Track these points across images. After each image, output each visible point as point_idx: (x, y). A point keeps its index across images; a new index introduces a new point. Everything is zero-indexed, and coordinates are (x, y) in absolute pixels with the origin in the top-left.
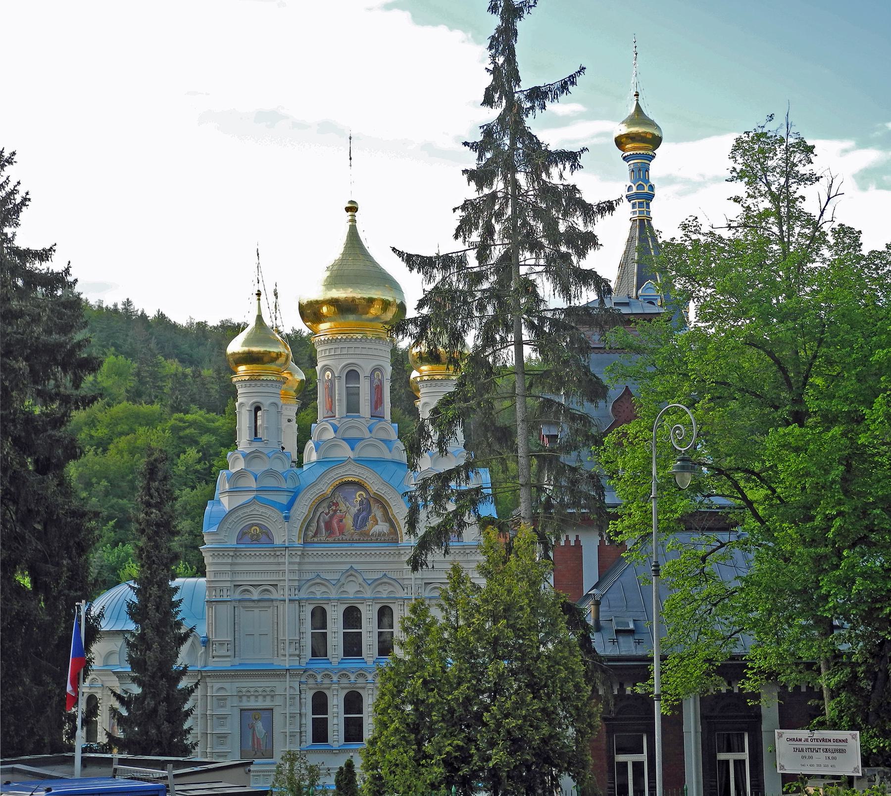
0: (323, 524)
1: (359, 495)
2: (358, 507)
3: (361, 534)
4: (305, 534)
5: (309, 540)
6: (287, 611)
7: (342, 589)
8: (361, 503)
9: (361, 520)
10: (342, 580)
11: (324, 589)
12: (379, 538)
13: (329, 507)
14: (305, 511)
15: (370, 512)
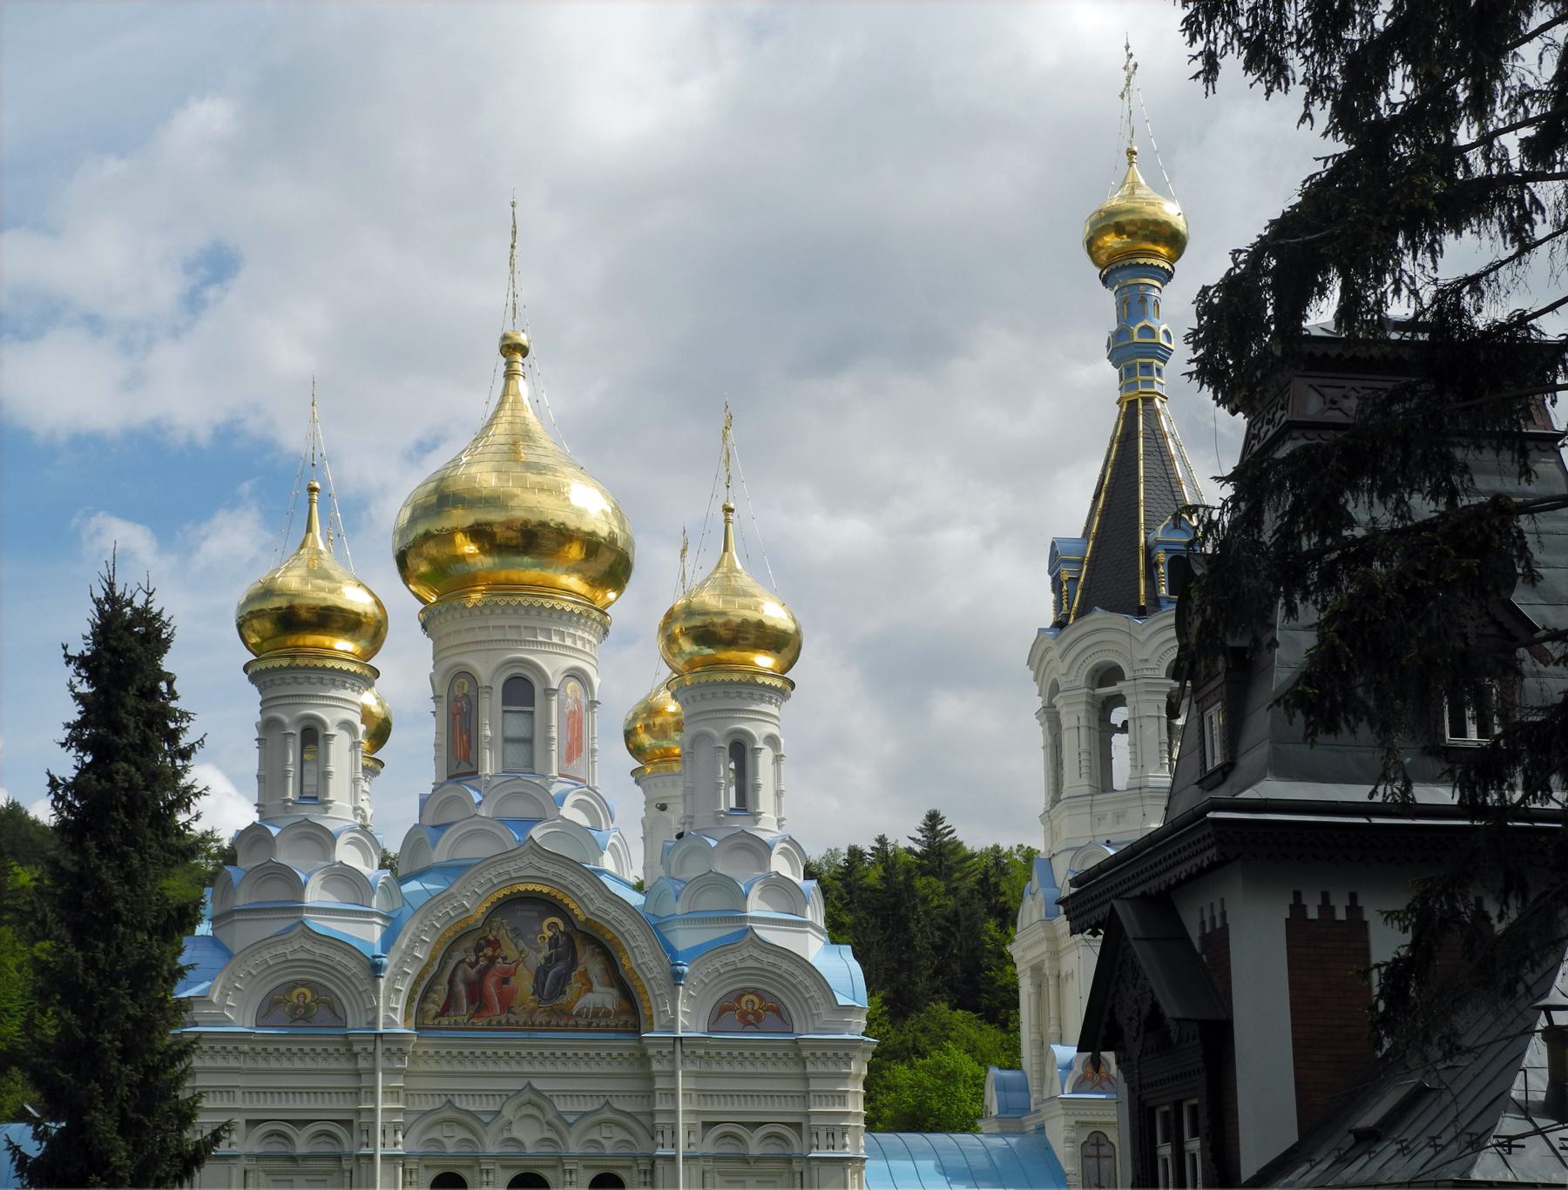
0: (461, 988)
1: (548, 927)
2: (546, 952)
3: (553, 1012)
4: (420, 1010)
5: (429, 1022)
7: (506, 1135)
8: (553, 943)
9: (552, 983)
10: (508, 1113)
11: (462, 1134)
12: (594, 1021)
13: (478, 949)
15: (574, 964)
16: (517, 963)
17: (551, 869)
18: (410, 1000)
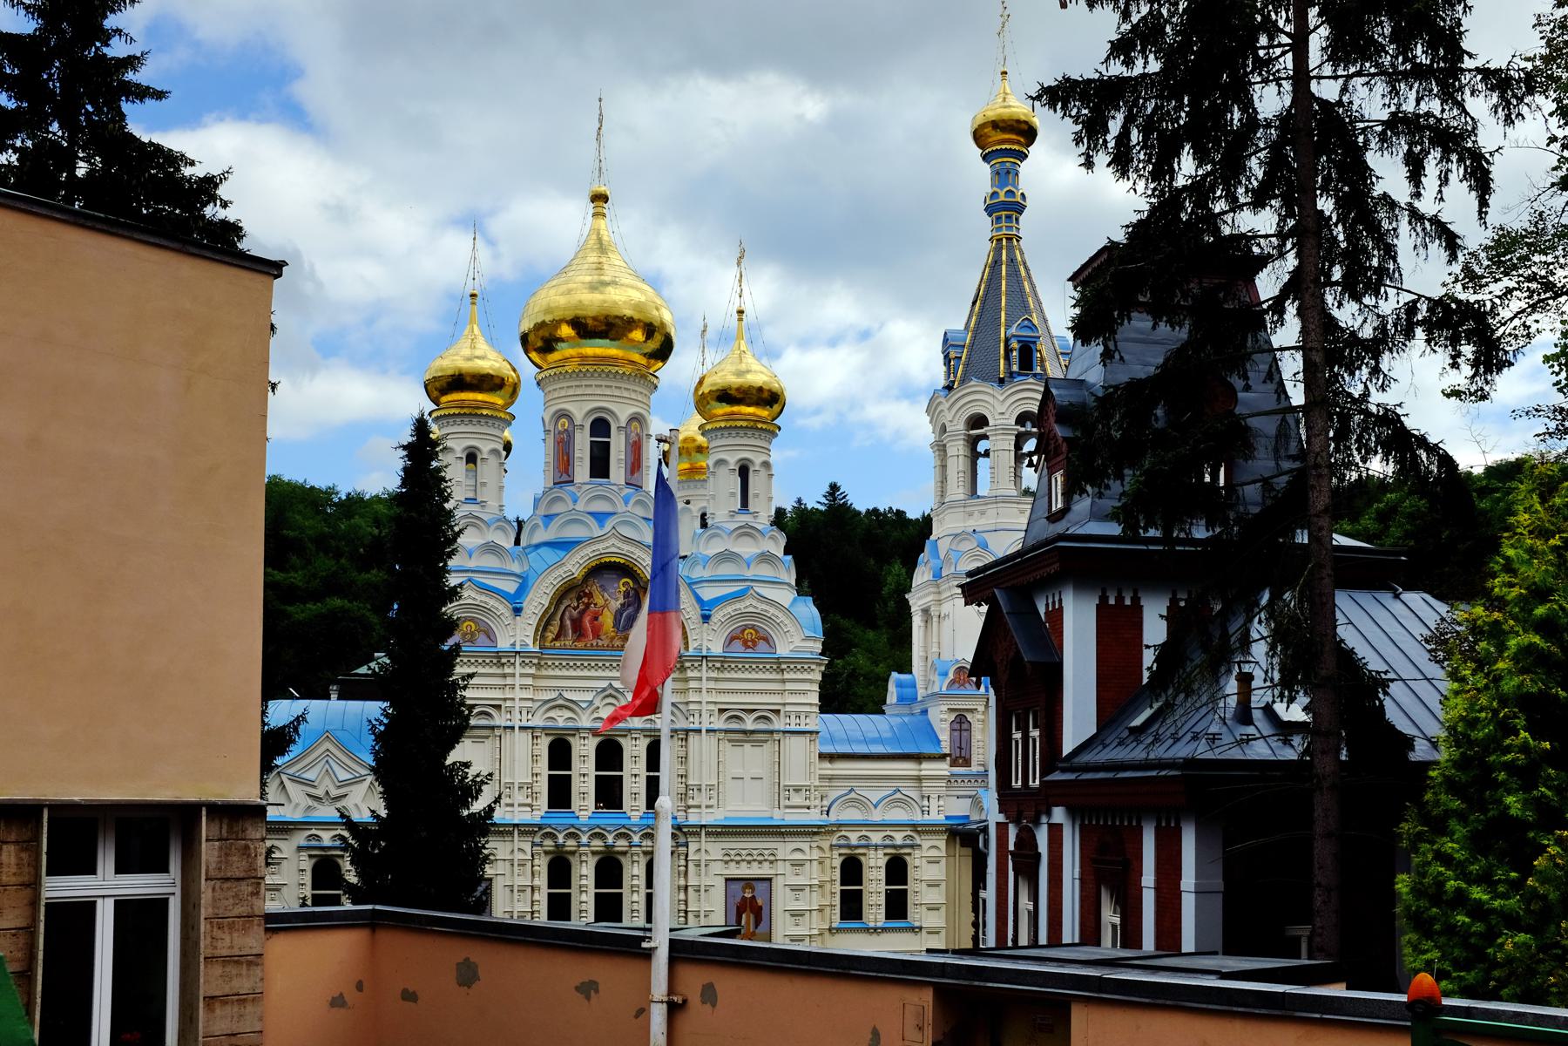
0: (568, 622)
2: (621, 600)
4: (542, 636)
6: (520, 744)
10: (597, 703)
11: (569, 714)
14: (546, 602)
16: (604, 607)
17: (626, 548)
18: (537, 630)
